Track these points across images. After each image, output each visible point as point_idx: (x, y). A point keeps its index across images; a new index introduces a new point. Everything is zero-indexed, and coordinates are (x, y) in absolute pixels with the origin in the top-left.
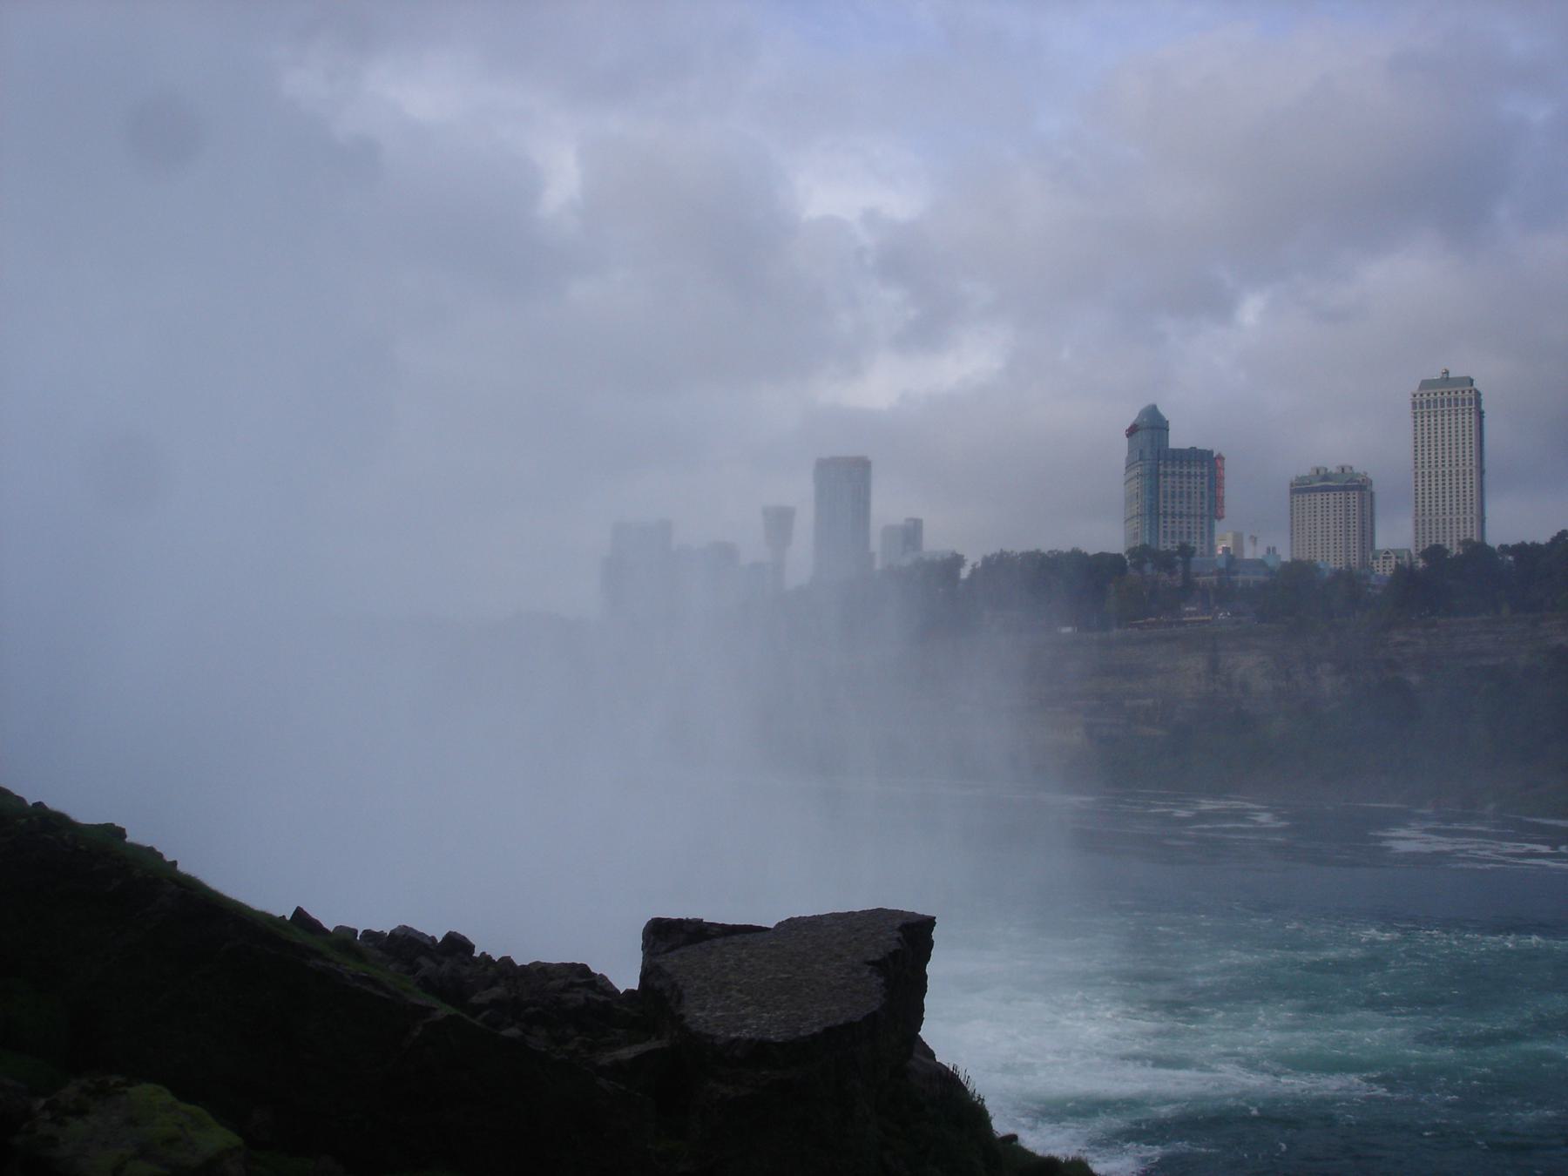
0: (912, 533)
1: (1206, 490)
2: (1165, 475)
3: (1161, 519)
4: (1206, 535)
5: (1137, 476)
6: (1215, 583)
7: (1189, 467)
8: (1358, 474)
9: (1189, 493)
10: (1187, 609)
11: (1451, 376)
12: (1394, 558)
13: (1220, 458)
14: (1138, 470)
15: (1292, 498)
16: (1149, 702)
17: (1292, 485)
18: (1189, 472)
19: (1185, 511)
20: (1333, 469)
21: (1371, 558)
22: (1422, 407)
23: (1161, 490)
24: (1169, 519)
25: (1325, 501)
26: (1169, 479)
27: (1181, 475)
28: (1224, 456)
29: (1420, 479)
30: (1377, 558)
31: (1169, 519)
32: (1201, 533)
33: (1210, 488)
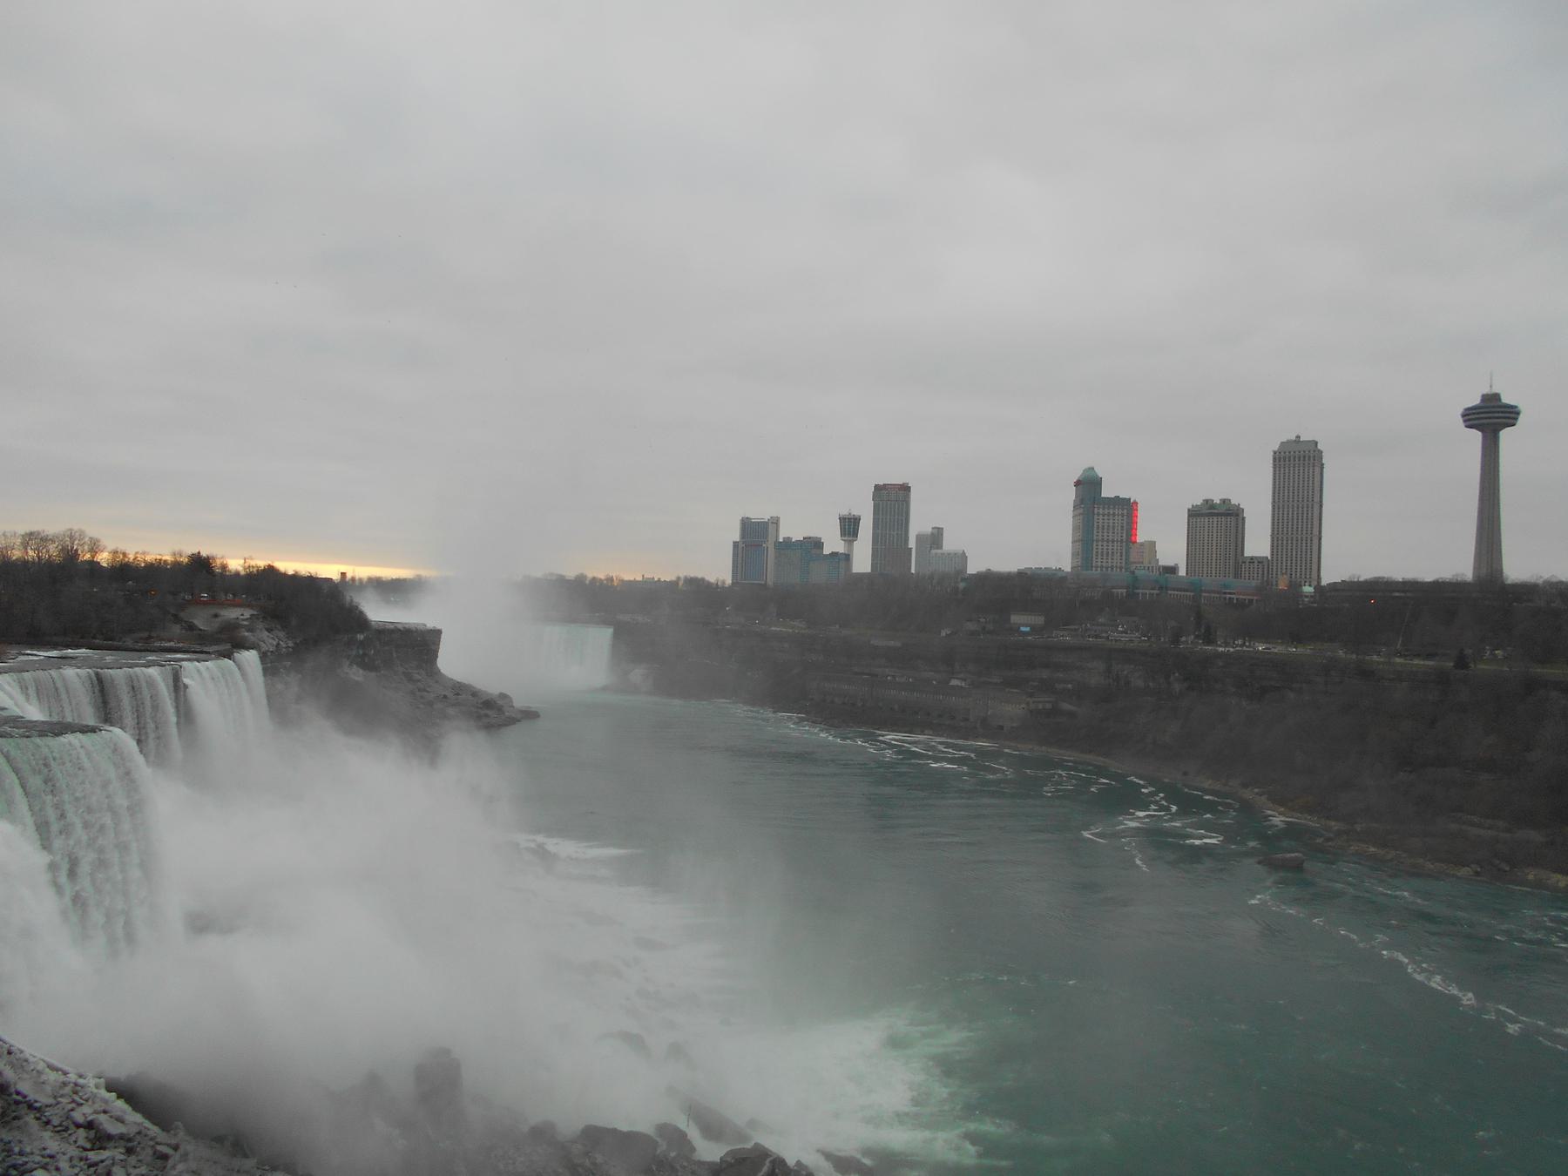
0: (936, 537)
1: (1125, 525)
2: (1098, 514)
3: (1095, 544)
4: (1124, 553)
5: (1080, 514)
6: (1124, 594)
7: (1114, 509)
8: (1235, 505)
9: (1114, 527)
10: (1101, 620)
11: (1301, 440)
12: (1256, 562)
13: (1136, 503)
14: (1081, 511)
15: (1189, 520)
16: (1070, 686)
17: (1189, 510)
18: (1114, 513)
19: (1111, 538)
20: (1217, 501)
21: (1240, 561)
22: (1280, 461)
23: (1096, 524)
24: (1100, 543)
25: (1211, 523)
26: (1101, 517)
27: (1109, 514)
28: (1138, 501)
29: (1276, 510)
30: (1245, 562)
31: (1100, 543)
32: (1121, 553)
33: (1128, 523)
